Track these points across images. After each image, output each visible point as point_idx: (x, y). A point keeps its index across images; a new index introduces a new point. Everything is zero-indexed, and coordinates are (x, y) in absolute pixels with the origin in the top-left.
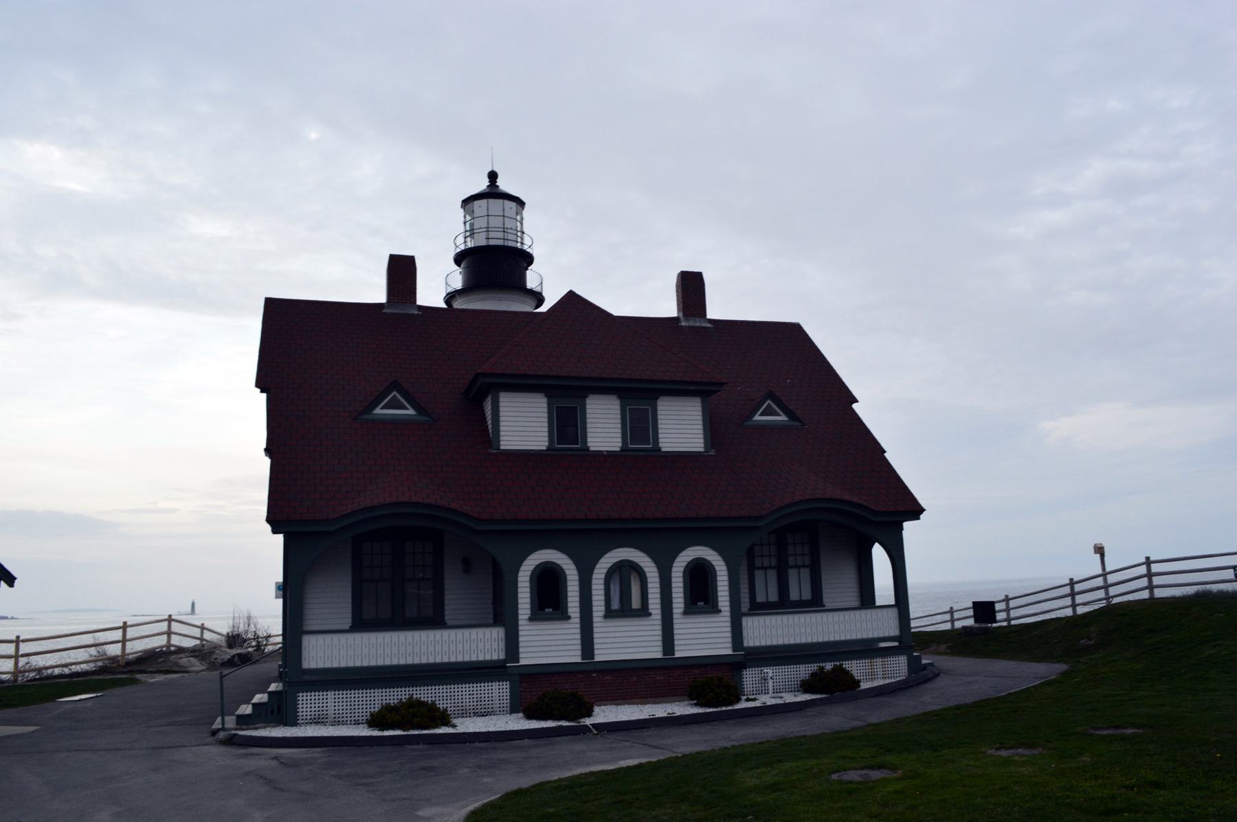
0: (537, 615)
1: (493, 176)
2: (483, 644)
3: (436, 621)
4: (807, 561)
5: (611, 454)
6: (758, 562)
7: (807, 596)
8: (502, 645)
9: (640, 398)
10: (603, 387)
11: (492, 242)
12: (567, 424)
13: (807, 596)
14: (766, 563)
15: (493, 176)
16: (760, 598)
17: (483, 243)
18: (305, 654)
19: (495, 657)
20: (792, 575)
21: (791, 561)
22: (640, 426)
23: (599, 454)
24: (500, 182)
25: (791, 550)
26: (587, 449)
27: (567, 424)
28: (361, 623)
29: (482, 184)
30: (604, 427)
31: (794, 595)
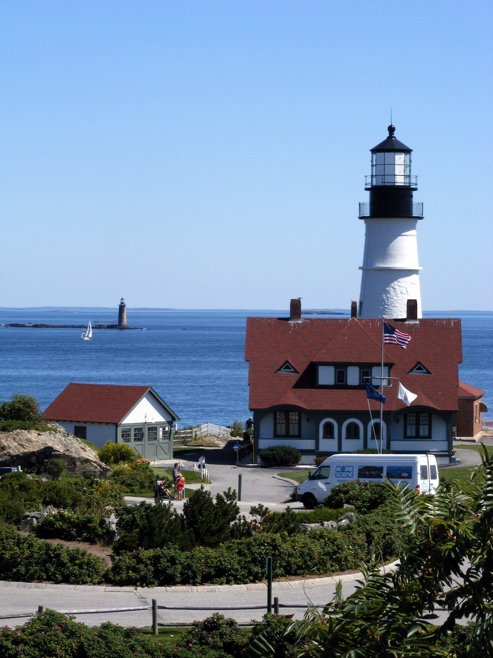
0: (325, 437)
1: (391, 129)
2: (308, 444)
3: (299, 436)
4: (427, 422)
6: (408, 422)
7: (426, 434)
8: (314, 445)
11: (386, 184)
13: (426, 434)
14: (411, 422)
15: (391, 129)
16: (409, 434)
17: (380, 184)
18: (259, 445)
19: (312, 448)
20: (421, 427)
21: (421, 422)
24: (396, 134)
25: (421, 419)
26: (347, 384)
29: (386, 135)
31: (421, 434)
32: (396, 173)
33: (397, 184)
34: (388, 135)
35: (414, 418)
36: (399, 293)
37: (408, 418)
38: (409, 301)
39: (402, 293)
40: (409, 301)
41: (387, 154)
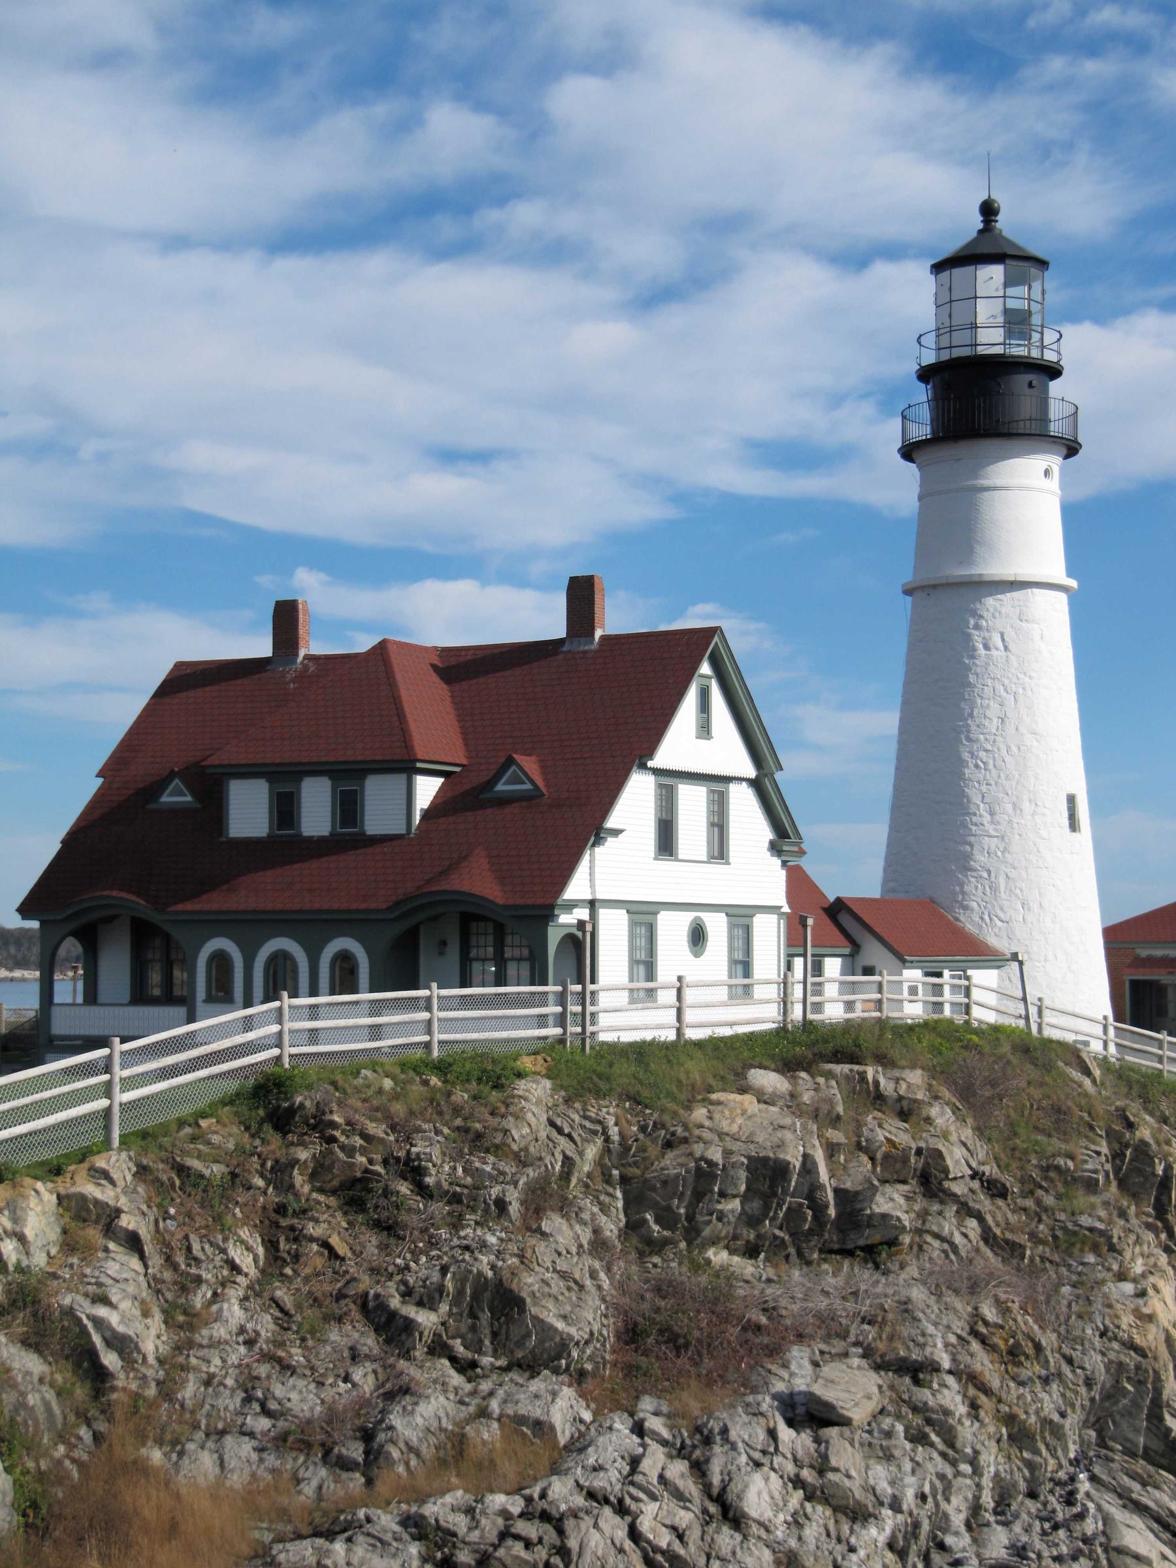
0: (210, 999)
1: (989, 210)
5: (321, 840)
10: (316, 771)
11: (957, 353)
12: (285, 809)
15: (989, 210)
22: (348, 808)
23: (310, 840)
24: (1004, 223)
25: (509, 939)
27: (285, 809)
28: (140, 996)
30: (316, 813)
32: (980, 320)
33: (981, 350)
34: (981, 226)
35: (490, 938)
36: (981, 646)
37: (473, 940)
38: (572, 579)
39: (987, 647)
40: (572, 579)
41: (958, 272)
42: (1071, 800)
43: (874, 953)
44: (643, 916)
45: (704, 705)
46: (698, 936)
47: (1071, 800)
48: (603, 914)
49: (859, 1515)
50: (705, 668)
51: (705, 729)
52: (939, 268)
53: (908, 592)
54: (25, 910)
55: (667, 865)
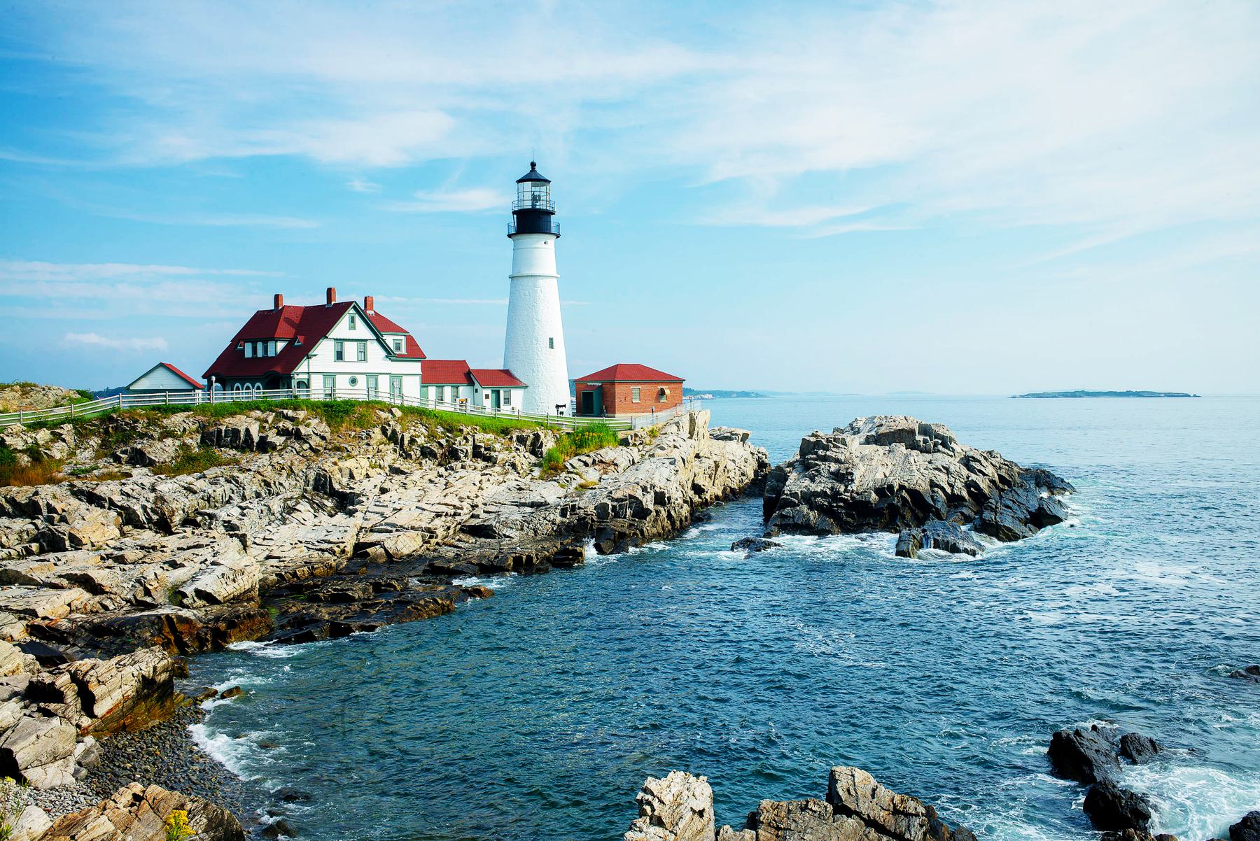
1: (533, 165)
9: (265, 342)
12: (255, 350)
15: (533, 165)
22: (265, 350)
27: (255, 350)
42: (551, 339)
43: (477, 386)
44: (330, 376)
45: (353, 320)
46: (354, 381)
47: (551, 339)
48: (313, 376)
49: (195, 492)
50: (352, 311)
51: (353, 327)
52: (519, 181)
53: (512, 278)
54: (204, 377)
55: (340, 363)
